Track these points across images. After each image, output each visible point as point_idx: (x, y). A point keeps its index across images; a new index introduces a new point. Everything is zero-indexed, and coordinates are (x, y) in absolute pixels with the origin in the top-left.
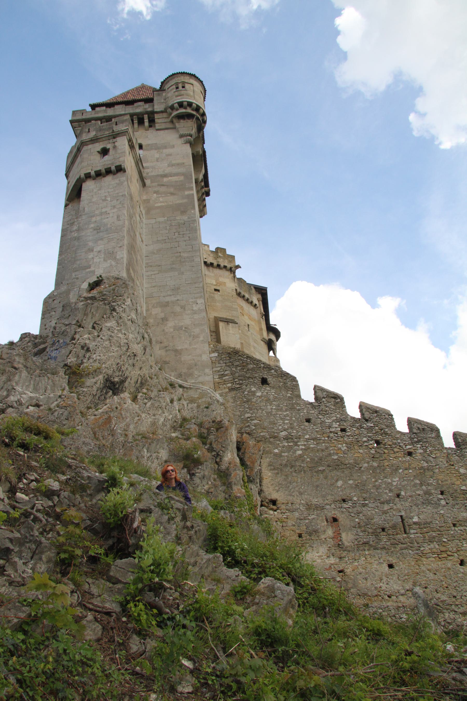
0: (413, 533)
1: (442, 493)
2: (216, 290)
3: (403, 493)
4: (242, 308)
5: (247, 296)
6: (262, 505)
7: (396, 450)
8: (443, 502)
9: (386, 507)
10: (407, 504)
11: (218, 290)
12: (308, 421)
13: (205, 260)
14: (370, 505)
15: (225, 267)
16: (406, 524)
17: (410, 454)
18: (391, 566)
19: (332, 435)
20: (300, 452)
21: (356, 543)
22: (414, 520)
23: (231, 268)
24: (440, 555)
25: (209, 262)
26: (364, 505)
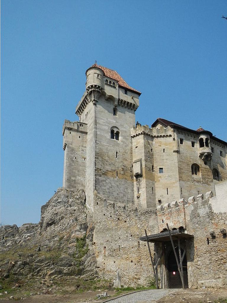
0: (121, 252)
1: (131, 236)
2: (136, 147)
3: (121, 237)
4: (160, 142)
5: (162, 135)
6: (93, 244)
7: (122, 221)
8: (131, 239)
9: (116, 242)
10: (121, 241)
11: (137, 147)
12: (104, 215)
13: (132, 136)
14: (113, 242)
15: (139, 134)
16: (120, 248)
17: (126, 221)
18: (115, 262)
19: (108, 219)
20: (101, 226)
21: (108, 255)
22: (122, 247)
23: (142, 133)
24: (127, 259)
25: (133, 136)
26: (112, 242)
